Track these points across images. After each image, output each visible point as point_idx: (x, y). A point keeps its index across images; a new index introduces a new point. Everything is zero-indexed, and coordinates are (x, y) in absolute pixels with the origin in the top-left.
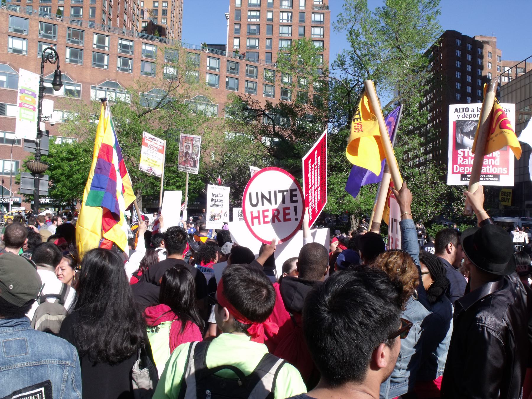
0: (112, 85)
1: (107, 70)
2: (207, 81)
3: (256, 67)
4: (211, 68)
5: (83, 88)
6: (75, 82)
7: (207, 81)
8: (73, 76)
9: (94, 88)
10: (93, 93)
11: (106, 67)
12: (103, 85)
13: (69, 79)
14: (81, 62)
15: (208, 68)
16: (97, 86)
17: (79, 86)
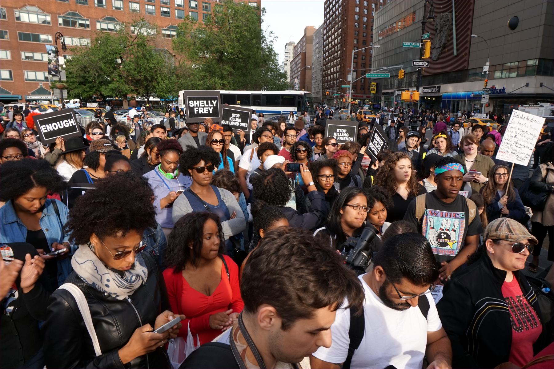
0: (110, 19)
1: (106, 10)
2: (176, 15)
3: (209, 4)
4: (178, 5)
5: (91, 22)
6: (85, 18)
7: (176, 15)
8: (83, 13)
9: (98, 21)
10: (98, 25)
11: (105, 7)
12: (104, 19)
13: (80, 16)
14: (87, 4)
15: (176, 5)
16: (100, 20)
17: (88, 20)
